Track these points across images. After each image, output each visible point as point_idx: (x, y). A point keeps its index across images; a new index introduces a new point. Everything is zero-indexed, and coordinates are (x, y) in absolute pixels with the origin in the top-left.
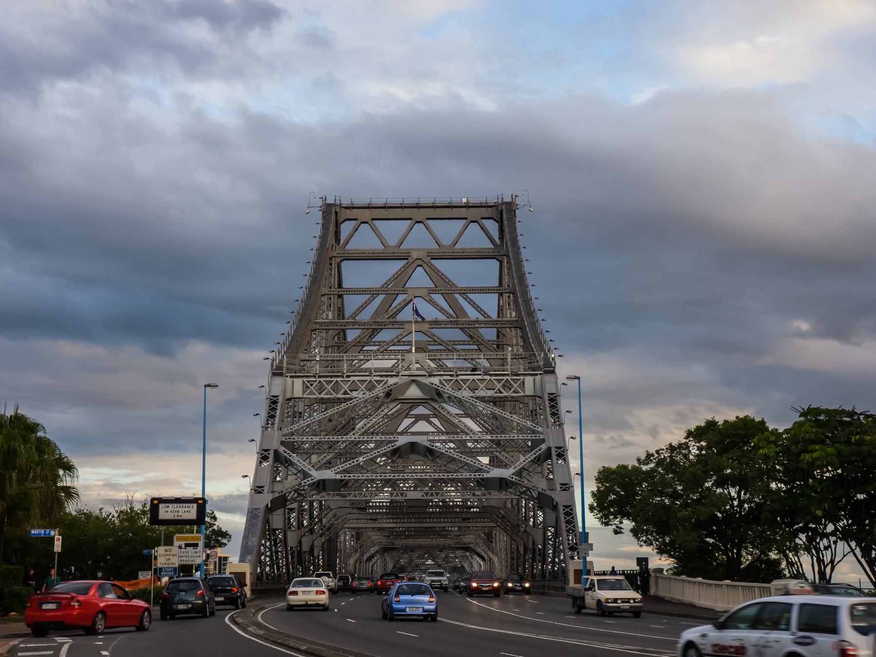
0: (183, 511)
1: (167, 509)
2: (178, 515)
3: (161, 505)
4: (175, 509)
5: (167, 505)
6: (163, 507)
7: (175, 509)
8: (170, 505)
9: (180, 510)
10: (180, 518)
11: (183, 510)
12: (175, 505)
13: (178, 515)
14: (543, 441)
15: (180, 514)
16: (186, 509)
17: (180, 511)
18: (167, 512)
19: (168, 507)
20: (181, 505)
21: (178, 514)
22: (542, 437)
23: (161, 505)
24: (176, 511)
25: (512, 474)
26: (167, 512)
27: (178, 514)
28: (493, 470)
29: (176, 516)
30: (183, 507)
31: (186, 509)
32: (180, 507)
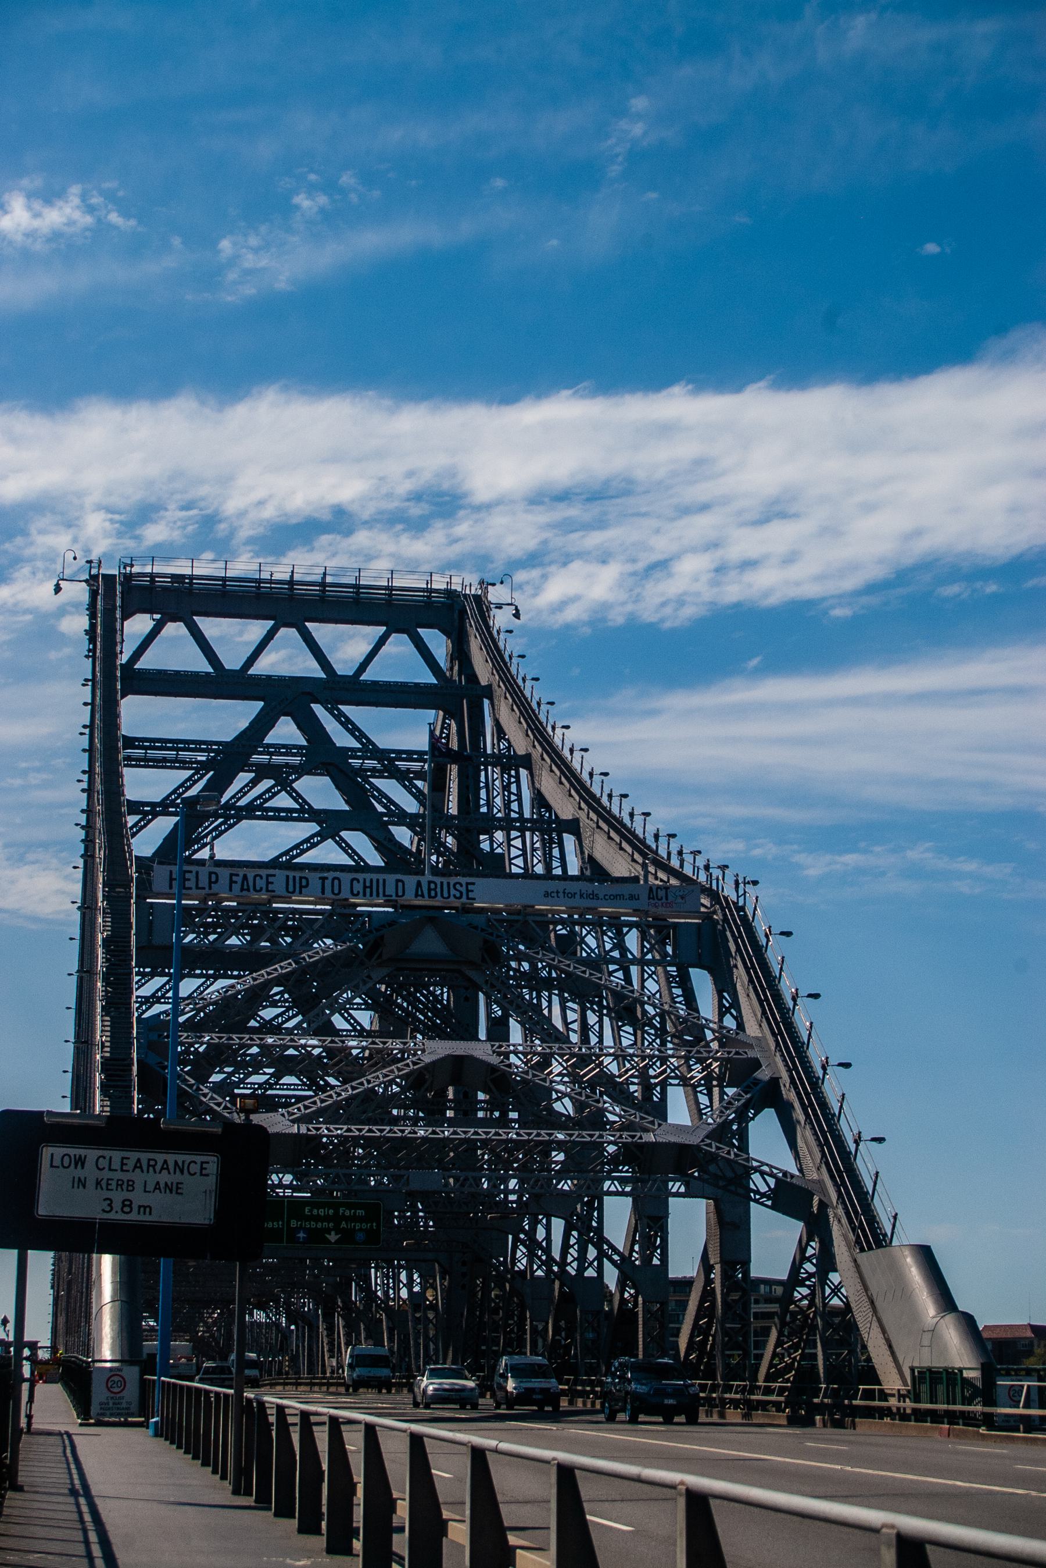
0: (150, 1187)
1: (79, 1173)
2: (127, 1204)
3: (47, 1152)
4: (119, 1175)
5: (73, 1152)
6: (57, 1162)
7: (119, 1175)
8: (91, 1154)
9: (138, 1177)
10: (134, 1216)
11: (152, 1179)
12: (116, 1155)
13: (127, 1204)
14: (756, 1064)
15: (138, 1197)
16: (164, 1178)
17: (139, 1186)
18: (82, 1183)
19: (80, 1161)
20: (144, 1157)
21: (130, 1195)
22: (751, 1054)
23: (47, 1152)
24: (120, 1184)
25: (707, 1137)
26: (82, 1183)
27: (130, 1195)
28: (660, 1125)
29: (117, 1205)
30: (151, 1165)
31: (164, 1178)
32: (138, 1165)
